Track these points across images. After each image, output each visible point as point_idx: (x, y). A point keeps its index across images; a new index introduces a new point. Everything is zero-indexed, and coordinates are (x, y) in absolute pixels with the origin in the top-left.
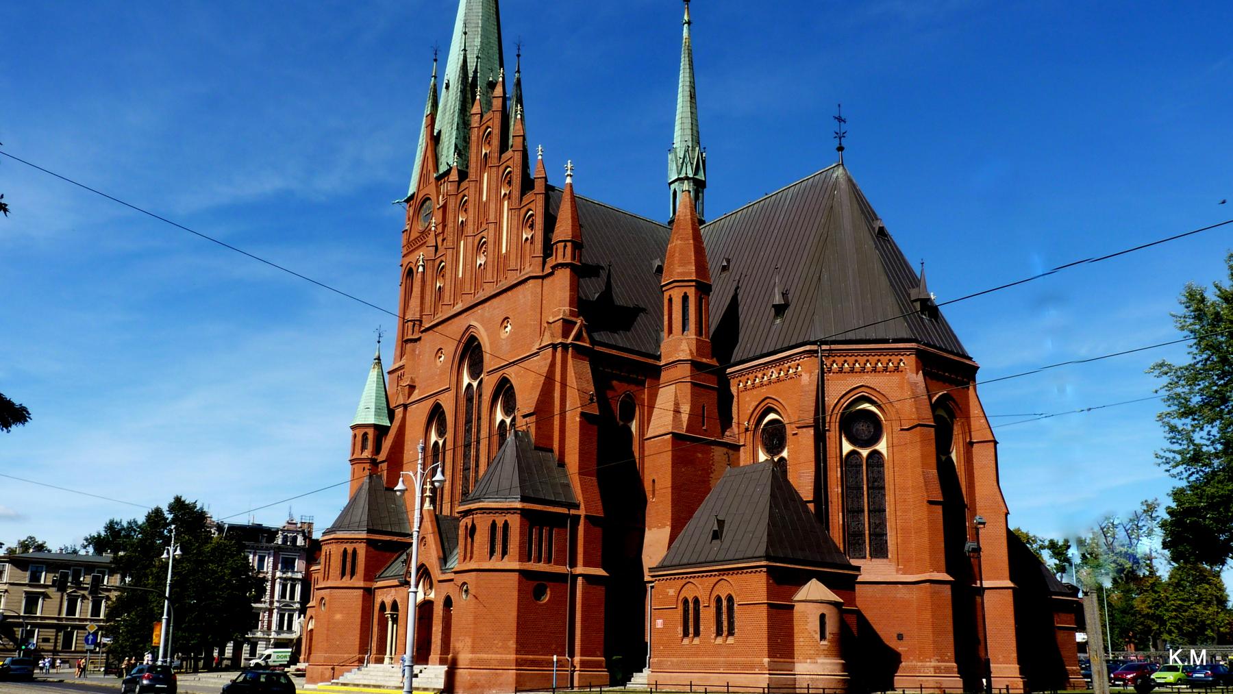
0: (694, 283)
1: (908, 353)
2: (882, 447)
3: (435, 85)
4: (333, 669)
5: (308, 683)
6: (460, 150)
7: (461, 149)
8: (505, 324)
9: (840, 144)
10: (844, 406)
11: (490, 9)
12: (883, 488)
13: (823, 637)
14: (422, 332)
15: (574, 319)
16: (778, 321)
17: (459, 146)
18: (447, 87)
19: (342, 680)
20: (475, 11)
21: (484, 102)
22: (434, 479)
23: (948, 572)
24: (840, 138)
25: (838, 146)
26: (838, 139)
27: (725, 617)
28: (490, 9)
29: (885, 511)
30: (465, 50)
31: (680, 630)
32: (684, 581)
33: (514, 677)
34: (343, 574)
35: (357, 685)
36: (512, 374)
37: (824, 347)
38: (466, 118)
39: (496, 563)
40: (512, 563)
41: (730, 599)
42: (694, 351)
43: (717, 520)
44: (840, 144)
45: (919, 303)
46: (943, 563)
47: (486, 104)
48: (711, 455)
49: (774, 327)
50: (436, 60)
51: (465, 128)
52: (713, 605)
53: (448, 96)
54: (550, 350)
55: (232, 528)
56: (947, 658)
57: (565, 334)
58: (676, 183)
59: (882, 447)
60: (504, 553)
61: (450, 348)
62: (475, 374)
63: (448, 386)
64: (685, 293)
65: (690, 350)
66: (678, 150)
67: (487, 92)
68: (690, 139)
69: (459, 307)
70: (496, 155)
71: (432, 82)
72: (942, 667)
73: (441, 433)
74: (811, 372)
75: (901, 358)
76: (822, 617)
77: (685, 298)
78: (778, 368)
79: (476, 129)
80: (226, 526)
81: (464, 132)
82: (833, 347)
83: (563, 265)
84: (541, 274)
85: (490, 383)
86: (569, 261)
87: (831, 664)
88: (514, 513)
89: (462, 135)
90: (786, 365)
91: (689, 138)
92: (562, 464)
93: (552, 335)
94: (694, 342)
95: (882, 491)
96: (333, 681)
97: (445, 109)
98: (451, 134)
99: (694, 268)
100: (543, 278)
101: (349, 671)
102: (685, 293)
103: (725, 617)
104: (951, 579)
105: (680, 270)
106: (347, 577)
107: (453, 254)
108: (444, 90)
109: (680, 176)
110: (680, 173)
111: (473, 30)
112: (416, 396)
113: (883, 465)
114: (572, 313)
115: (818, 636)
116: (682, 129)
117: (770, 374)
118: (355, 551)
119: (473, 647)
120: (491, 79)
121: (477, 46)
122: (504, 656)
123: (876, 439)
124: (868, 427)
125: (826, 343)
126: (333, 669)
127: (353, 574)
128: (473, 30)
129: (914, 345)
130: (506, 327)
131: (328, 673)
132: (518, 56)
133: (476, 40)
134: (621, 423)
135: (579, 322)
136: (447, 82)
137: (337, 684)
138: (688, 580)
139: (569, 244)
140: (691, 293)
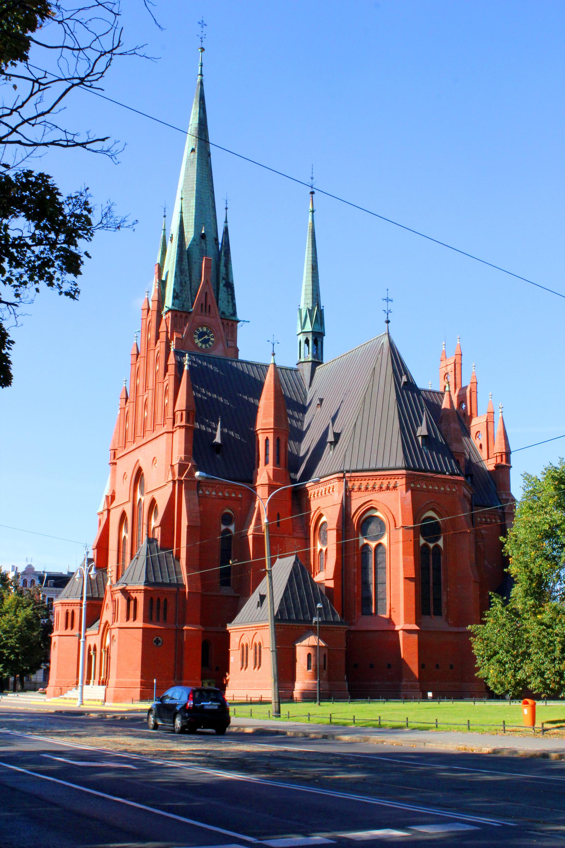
0: (272, 431)
1: (401, 477)
2: (384, 541)
3: (164, 237)
4: (61, 689)
5: (48, 698)
6: (177, 294)
7: (178, 292)
8: (155, 462)
9: (388, 318)
10: (360, 514)
11: (203, 174)
12: (385, 568)
13: (309, 667)
14: (117, 459)
15: (187, 463)
16: (331, 452)
17: (176, 290)
18: (171, 240)
19: (66, 696)
20: (191, 177)
21: (198, 251)
22: (90, 573)
23: (417, 624)
24: (388, 314)
25: (386, 319)
26: (386, 314)
27: (258, 655)
28: (203, 174)
29: (385, 583)
30: (181, 212)
31: (240, 663)
32: (241, 634)
33: (139, 692)
34: (66, 628)
35: (70, 699)
36: (156, 495)
37: (347, 475)
38: (182, 267)
39: (131, 624)
40: (139, 623)
41: (260, 644)
42: (272, 477)
43: (260, 595)
44: (388, 318)
45: (421, 437)
46: (413, 618)
47: (200, 253)
48: (284, 546)
49: (328, 456)
50: (165, 216)
51: (182, 275)
52: (253, 648)
53: (172, 247)
54: (171, 484)
55: (50, 577)
56: (412, 679)
57: (180, 474)
58: (301, 335)
59: (384, 541)
60: (135, 619)
61: (130, 473)
62: (142, 494)
63: (128, 500)
64: (267, 438)
65: (269, 477)
66: (302, 311)
67: (201, 243)
68: (311, 302)
69: (134, 446)
70: (153, 341)
71: (162, 234)
72: (409, 685)
73: (127, 532)
74: (339, 492)
75: (396, 480)
76: (309, 655)
77: (267, 440)
78: (325, 487)
79: (145, 320)
80: (46, 575)
81: (181, 278)
82: (354, 474)
83: (180, 427)
84: (171, 430)
85: (146, 500)
86: (183, 423)
87: (313, 683)
88: (140, 592)
89: (179, 281)
90: (328, 486)
91: (310, 301)
92: (178, 558)
93: (173, 474)
94: (272, 471)
95: (384, 570)
96: (60, 696)
97: (169, 259)
98: (171, 280)
99: (273, 419)
100: (173, 432)
101: (71, 690)
102: (267, 438)
103: (258, 655)
104: (417, 628)
105: (264, 421)
106: (69, 628)
107: (133, 406)
108: (170, 242)
109: (304, 331)
110: (303, 327)
111: (190, 193)
112: (114, 504)
113: (385, 553)
114: (186, 459)
115: (306, 667)
116: (306, 294)
117: (321, 491)
118: (73, 612)
119: (117, 674)
120: (203, 232)
121: (193, 206)
122: (134, 680)
123: (380, 536)
124: (377, 527)
125: (348, 472)
126: (61, 689)
127: (72, 627)
128: (190, 193)
129: (404, 472)
130: (155, 464)
131: (58, 691)
132: (227, 208)
133: (192, 201)
134: (223, 527)
135: (190, 464)
136: (171, 236)
137: (65, 698)
138: (244, 632)
139: (184, 413)
140: (271, 437)
